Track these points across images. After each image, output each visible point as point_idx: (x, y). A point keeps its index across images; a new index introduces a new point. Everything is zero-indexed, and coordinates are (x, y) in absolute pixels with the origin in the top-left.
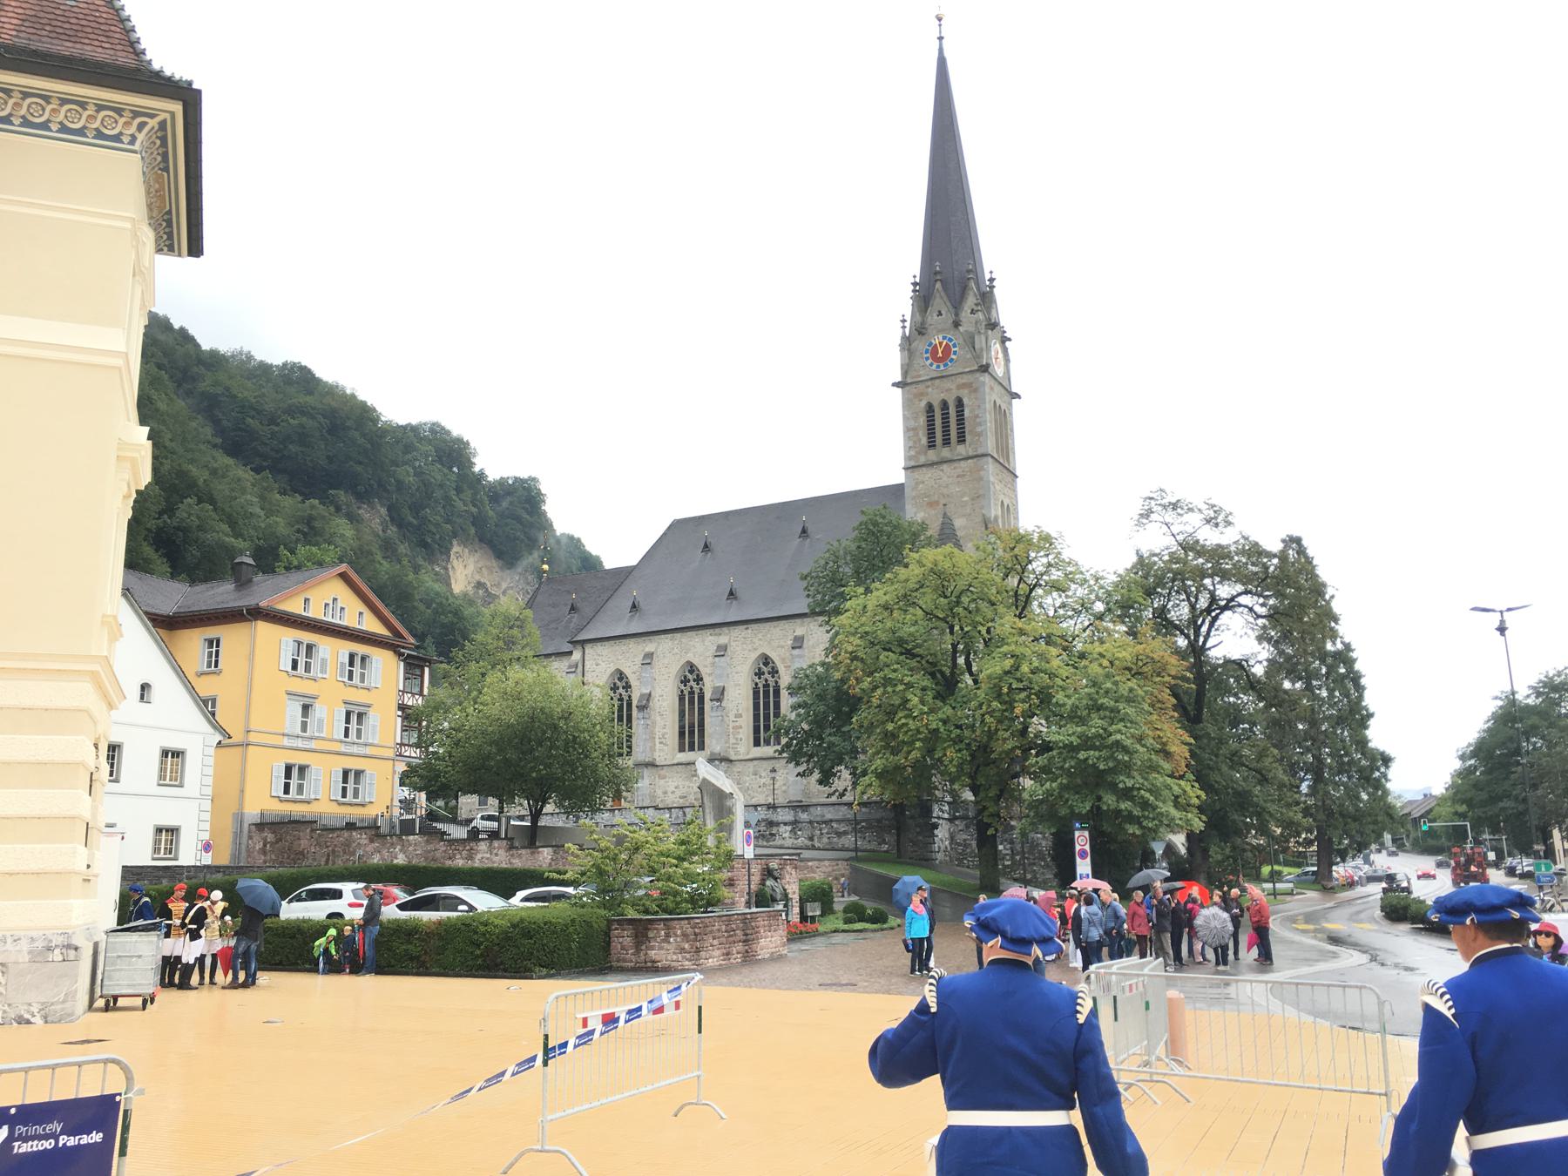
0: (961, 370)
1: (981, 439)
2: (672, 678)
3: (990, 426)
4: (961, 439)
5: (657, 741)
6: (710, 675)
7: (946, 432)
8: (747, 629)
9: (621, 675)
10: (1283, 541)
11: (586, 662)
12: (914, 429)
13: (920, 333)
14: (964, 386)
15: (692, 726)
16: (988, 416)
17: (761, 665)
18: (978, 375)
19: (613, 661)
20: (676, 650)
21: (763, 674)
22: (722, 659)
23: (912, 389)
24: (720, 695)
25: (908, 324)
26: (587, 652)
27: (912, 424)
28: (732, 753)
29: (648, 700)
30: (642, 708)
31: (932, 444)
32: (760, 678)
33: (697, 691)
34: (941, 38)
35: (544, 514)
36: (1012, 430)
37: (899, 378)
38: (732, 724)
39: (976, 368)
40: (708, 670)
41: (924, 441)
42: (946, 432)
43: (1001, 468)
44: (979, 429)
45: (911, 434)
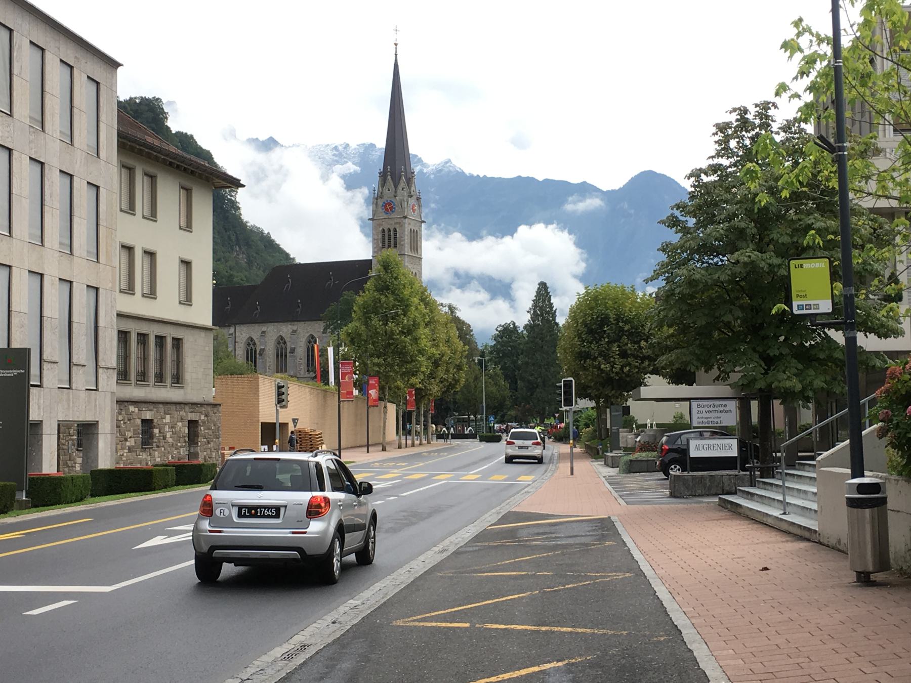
3: (407, 240)
4: (395, 246)
7: (390, 242)
9: (252, 339)
12: (377, 240)
14: (399, 223)
15: (282, 353)
16: (406, 237)
18: (403, 219)
20: (275, 330)
24: (293, 351)
25: (376, 192)
26: (237, 328)
27: (376, 237)
30: (260, 354)
31: (383, 246)
33: (284, 348)
34: (396, 55)
35: (168, 128)
36: (421, 238)
37: (371, 217)
41: (381, 245)
42: (390, 242)
44: (402, 243)
45: (376, 241)
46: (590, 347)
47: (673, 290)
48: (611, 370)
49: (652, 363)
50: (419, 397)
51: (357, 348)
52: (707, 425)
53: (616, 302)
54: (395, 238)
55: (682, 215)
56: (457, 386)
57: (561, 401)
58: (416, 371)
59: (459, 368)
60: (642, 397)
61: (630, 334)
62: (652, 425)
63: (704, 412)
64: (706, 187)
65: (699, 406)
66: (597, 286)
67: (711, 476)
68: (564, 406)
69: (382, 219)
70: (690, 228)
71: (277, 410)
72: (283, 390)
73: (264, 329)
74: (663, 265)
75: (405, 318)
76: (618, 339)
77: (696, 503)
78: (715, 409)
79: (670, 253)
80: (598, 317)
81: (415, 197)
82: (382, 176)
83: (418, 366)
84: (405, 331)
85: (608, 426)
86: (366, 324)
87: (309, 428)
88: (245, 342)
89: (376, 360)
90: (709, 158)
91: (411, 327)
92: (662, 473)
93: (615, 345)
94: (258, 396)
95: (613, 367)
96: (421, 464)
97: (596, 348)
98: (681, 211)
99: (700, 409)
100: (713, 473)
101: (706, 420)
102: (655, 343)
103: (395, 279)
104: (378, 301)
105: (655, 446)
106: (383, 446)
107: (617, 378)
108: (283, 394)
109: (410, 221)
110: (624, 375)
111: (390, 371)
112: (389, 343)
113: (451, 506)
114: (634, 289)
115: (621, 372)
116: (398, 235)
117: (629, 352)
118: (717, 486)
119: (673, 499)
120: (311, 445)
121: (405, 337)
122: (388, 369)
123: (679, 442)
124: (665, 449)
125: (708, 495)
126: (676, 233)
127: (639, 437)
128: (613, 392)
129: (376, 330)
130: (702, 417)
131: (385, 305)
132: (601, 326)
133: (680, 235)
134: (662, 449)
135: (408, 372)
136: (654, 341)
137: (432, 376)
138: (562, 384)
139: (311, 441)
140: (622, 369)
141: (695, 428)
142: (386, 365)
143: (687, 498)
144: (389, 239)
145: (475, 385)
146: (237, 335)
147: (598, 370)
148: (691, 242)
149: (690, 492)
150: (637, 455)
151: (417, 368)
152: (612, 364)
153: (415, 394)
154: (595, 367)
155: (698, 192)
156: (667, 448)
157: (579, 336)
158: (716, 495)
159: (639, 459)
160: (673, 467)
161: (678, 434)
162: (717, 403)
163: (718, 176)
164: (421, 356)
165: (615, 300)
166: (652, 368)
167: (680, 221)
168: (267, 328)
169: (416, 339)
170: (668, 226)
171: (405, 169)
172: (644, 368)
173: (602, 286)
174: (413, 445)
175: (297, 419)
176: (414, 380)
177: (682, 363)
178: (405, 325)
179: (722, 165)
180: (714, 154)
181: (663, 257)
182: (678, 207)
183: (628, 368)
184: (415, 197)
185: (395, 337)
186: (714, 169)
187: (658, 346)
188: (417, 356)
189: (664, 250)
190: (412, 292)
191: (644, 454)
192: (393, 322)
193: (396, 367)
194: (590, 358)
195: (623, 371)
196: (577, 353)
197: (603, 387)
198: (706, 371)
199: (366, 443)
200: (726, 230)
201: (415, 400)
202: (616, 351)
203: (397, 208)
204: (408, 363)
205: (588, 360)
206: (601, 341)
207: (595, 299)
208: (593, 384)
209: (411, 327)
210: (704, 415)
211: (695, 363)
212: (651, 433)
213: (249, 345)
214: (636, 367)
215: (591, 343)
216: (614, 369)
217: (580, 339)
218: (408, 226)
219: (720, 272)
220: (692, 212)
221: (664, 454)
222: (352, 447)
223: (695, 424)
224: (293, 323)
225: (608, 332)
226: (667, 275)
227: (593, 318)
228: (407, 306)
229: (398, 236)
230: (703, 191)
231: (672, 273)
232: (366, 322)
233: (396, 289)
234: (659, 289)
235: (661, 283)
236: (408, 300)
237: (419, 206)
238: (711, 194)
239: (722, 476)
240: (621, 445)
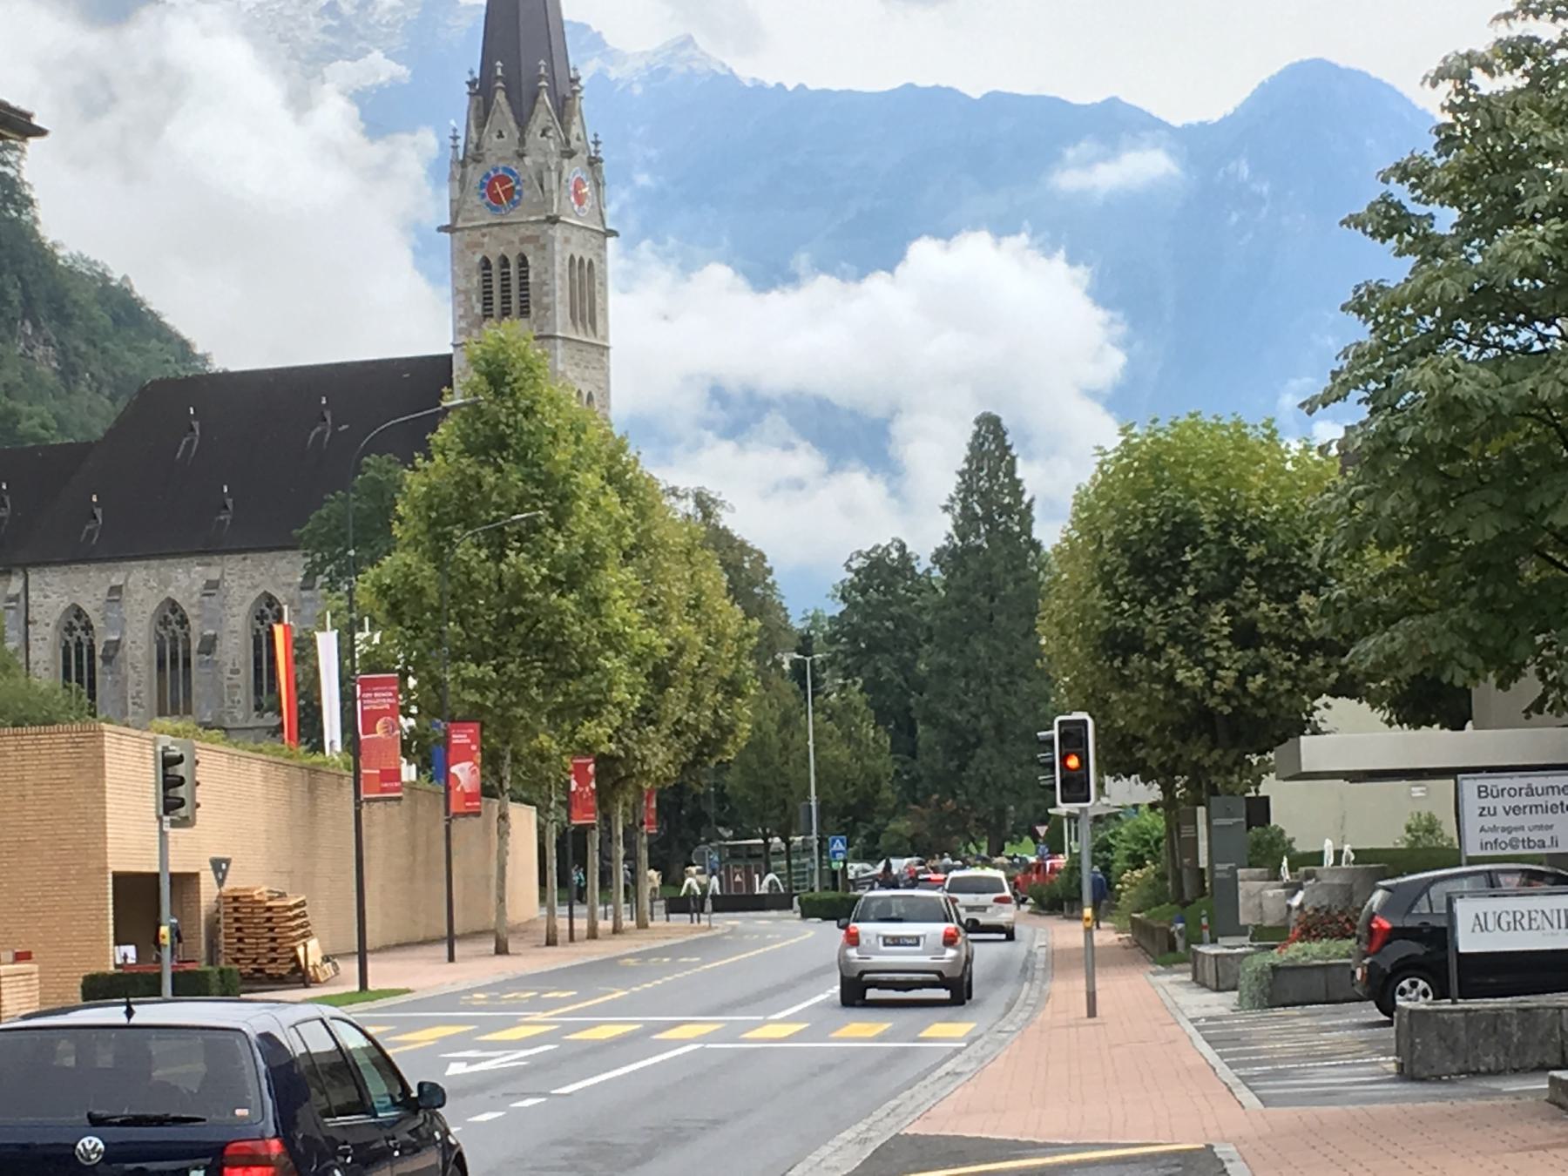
0: (524, 219)
1: (548, 314)
2: (146, 622)
4: (524, 312)
5: (130, 701)
6: (198, 617)
7: (506, 299)
8: (245, 559)
9: (79, 613)
10: (977, 422)
11: (30, 593)
12: (466, 292)
13: (477, 161)
16: (558, 282)
17: (264, 607)
18: (545, 226)
19: (66, 594)
21: (267, 617)
22: (213, 599)
23: (467, 237)
24: (209, 645)
25: (461, 142)
26: (31, 578)
27: (463, 284)
28: (227, 719)
29: (117, 650)
30: (107, 659)
31: (487, 314)
32: (262, 623)
36: (604, 284)
37: (447, 222)
38: (226, 683)
39: (543, 217)
40: (195, 611)
41: (478, 309)
42: (506, 299)
43: (580, 346)
44: (546, 300)
46: (1142, 614)
47: (1393, 434)
48: (1209, 685)
49: (1334, 660)
50: (609, 781)
51: (410, 633)
52: (1509, 851)
53: (1218, 475)
54: (524, 286)
55: (1417, 199)
56: (728, 747)
57: (1053, 787)
58: (598, 703)
59: (732, 688)
60: (1304, 769)
61: (1265, 573)
62: (1338, 854)
63: (1500, 810)
64: (1488, 110)
65: (1482, 792)
66: (1158, 425)
67: (1526, 1010)
68: (1064, 801)
69: (483, 226)
70: (1443, 238)
71: (163, 834)
72: (181, 770)
73: (116, 580)
74: (1361, 355)
75: (559, 537)
76: (1228, 592)
77: (1483, 1095)
78: (1535, 800)
79: (1381, 319)
80: (1162, 522)
81: (582, 157)
82: (478, 93)
83: (604, 684)
84: (561, 576)
85: (1203, 862)
86: (437, 557)
87: (264, 889)
88: (57, 628)
89: (472, 671)
90: (1497, 18)
91: (579, 562)
92: (1372, 1003)
93: (1218, 608)
94: (102, 789)
95: (1212, 675)
96: (620, 994)
97: (1158, 619)
98: (1413, 187)
99: (1489, 802)
100: (1532, 1001)
101: (1506, 837)
102: (1340, 598)
103: (526, 415)
104: (472, 484)
105: (1348, 920)
106: (498, 942)
107: (1227, 710)
108: (181, 781)
109: (567, 233)
110: (1248, 702)
111: (517, 704)
112: (510, 614)
113: (716, 1122)
114: (1275, 432)
115: (1238, 691)
116: (531, 275)
117: (1262, 628)
118: (1542, 1043)
119: (1407, 1085)
120: (273, 940)
121: (562, 595)
122: (511, 696)
123: (1423, 907)
124: (1381, 928)
125: (1516, 1071)
126: (1400, 254)
127: (1300, 896)
128: (1216, 754)
129: (469, 574)
130: (1494, 829)
131: (495, 497)
132: (1174, 550)
133: (1411, 260)
134: (1371, 931)
135: (573, 706)
136: (1336, 593)
137: (647, 715)
138: (1056, 732)
139: (271, 930)
140: (1241, 680)
141: (1472, 861)
142: (504, 684)
143: (1450, 1081)
144: (505, 288)
145: (783, 741)
146: (30, 602)
147: (1166, 688)
148: (1447, 280)
149: (1460, 1064)
150: (1296, 951)
151: (601, 691)
152: (1210, 666)
153: (597, 773)
154: (1157, 677)
155: (1463, 124)
156: (1387, 925)
157: (1107, 581)
158: (1543, 1068)
159: (1302, 961)
160: (1405, 984)
161: (1421, 880)
162: (1539, 781)
163: (1526, 73)
164: (610, 654)
165: (1216, 468)
166: (1335, 675)
167: (1409, 216)
168: (129, 574)
169: (595, 601)
170: (1372, 235)
171: (551, 68)
172: (1311, 678)
173: (1173, 425)
174: (593, 934)
175: (227, 861)
176: (590, 730)
177: (1425, 659)
178: (560, 556)
179: (1538, 41)
180: (1511, 8)
181: (1361, 332)
182: (1402, 171)
183: (1260, 679)
184: (582, 157)
185: (528, 596)
186: (1516, 52)
187: (1351, 605)
188: (599, 653)
189: (1360, 308)
190: (580, 454)
191: (1315, 947)
192: (519, 550)
193: (534, 691)
194: (1139, 649)
195: (1245, 689)
196: (1100, 635)
197: (1184, 741)
198: (1502, 685)
199: (445, 932)
200: (1556, 243)
201: (598, 792)
202: (1223, 625)
203: (526, 193)
204: (569, 675)
205: (1135, 657)
206: (1173, 593)
207: (1154, 463)
208: (1153, 727)
209: (579, 562)
210: (1502, 820)
211: (1466, 658)
212: (1337, 881)
213: (70, 629)
214: (1285, 674)
215: (1143, 602)
216: (1216, 684)
217: (1109, 592)
218: (564, 247)
219: (1537, 374)
220: (1446, 189)
221: (1378, 940)
222: (400, 946)
223: (1472, 850)
224: (207, 559)
225: (1196, 565)
226: (1372, 386)
227: (1146, 525)
228: (564, 498)
229: (531, 280)
230: (1478, 123)
231: (1388, 381)
232: (438, 546)
233: (526, 448)
234: (1346, 428)
235: (1356, 409)
236: (566, 479)
237: (598, 185)
238: (1502, 133)
239: (1560, 1008)
240: (1242, 922)
